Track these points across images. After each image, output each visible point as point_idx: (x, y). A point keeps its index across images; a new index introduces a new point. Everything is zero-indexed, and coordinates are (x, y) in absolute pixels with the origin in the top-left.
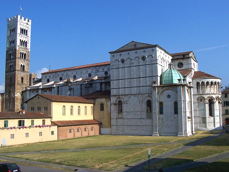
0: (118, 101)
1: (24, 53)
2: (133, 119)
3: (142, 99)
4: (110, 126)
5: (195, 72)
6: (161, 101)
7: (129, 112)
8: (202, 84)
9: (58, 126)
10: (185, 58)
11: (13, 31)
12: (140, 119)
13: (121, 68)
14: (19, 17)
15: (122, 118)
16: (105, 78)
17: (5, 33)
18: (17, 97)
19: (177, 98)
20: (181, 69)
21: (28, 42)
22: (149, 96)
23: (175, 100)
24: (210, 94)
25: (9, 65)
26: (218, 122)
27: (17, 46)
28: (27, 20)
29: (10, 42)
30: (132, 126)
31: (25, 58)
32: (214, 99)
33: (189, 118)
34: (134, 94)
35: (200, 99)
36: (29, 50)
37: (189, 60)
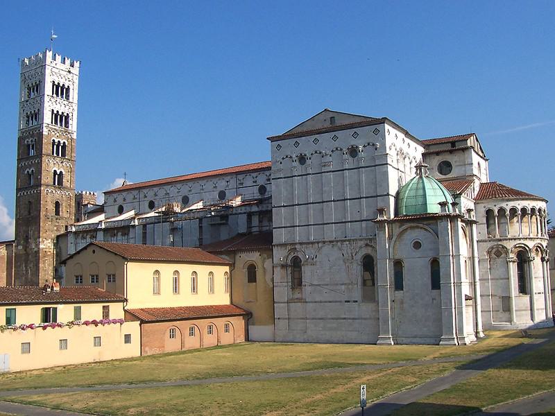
0: (290, 257)
1: (62, 142)
2: (330, 302)
3: (349, 252)
4: (273, 319)
5: (482, 185)
6: (397, 257)
7: (319, 285)
8: (502, 213)
9: (142, 322)
10: (455, 150)
11: (34, 89)
12: (346, 302)
13: (299, 176)
14: (49, 54)
15: (300, 300)
16: (260, 202)
17: (16, 93)
18: (44, 250)
19: (437, 250)
20: (448, 176)
21: (70, 115)
22: (367, 245)
23: (431, 255)
24: (520, 239)
25: (26, 172)
26: (541, 309)
27: (45, 125)
28: (68, 62)
29: (28, 117)
30: (327, 319)
31: (63, 155)
32: (530, 250)
33: (468, 298)
34: (330, 242)
35: (494, 250)
36: (75, 136)
37: (466, 155)
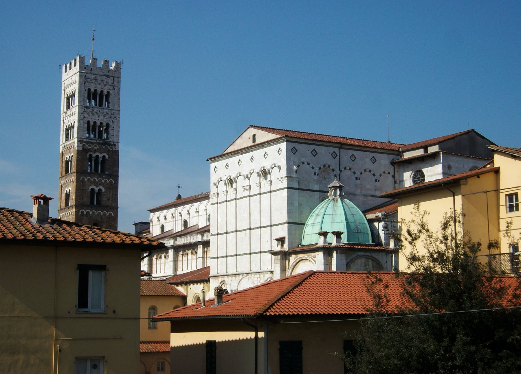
1: (101, 156)
